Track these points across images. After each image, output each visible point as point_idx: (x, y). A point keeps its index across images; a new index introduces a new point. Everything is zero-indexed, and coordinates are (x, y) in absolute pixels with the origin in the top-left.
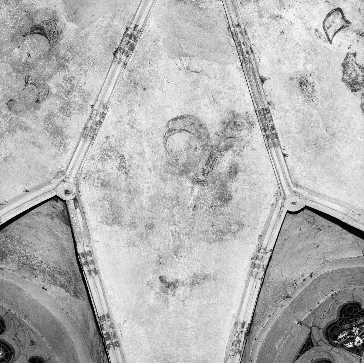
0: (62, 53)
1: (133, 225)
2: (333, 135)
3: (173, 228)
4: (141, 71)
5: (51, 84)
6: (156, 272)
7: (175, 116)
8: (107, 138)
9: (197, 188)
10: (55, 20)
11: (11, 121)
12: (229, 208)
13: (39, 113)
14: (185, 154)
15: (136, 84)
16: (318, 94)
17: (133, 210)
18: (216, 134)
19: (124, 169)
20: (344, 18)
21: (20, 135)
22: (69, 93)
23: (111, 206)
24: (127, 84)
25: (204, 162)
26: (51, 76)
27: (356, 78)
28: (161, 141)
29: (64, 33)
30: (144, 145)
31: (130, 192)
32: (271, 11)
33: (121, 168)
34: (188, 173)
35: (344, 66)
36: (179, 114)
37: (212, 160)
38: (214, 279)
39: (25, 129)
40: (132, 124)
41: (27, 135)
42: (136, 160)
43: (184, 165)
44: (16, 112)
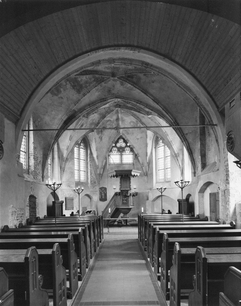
1: (131, 134)
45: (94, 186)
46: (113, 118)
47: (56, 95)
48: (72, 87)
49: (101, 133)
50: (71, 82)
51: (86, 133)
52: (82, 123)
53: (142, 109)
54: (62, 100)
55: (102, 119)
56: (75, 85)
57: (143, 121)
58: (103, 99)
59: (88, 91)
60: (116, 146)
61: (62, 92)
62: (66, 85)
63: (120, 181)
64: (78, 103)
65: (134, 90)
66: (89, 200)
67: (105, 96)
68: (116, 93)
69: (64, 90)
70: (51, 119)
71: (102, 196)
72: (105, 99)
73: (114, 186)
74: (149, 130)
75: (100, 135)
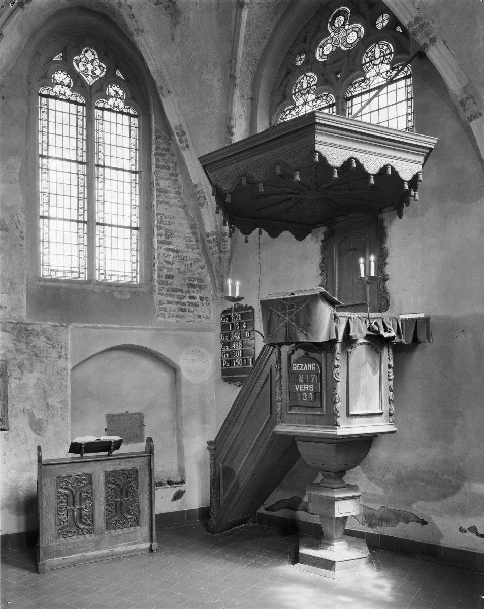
45: (187, 300)
60: (311, 64)
63: (321, 257)
66: (163, 376)
71: (231, 354)
73: (229, 281)
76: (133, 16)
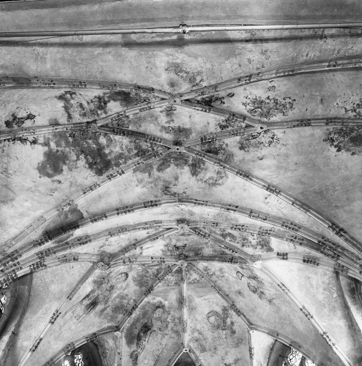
0: (167, 310)
1: (210, 350)
2: (255, 307)
3: (222, 347)
4: (192, 304)
5: (168, 320)
6: (223, 363)
7: (208, 313)
8: (191, 327)
9: (224, 332)
10: (161, 303)
11: (162, 334)
12: (236, 335)
13: (169, 329)
14: (216, 322)
15: (192, 308)
16: (245, 295)
17: (208, 345)
18: (222, 314)
19: (200, 333)
20: (241, 274)
21: (166, 337)
22: (174, 320)
23: (201, 346)
24: (189, 310)
25: (222, 323)
26: (167, 317)
27: (253, 289)
28: (207, 321)
29: (166, 304)
30: (203, 324)
31: (205, 340)
32: (220, 275)
33: (199, 333)
34: (219, 328)
35: (248, 286)
36: (209, 312)
37: (224, 322)
38: (241, 360)
39: (167, 334)
40: (196, 320)
41: (168, 336)
42: (202, 329)
43: (217, 325)
44: (163, 331)
46: (169, 298)
47: (49, 176)
48: (87, 166)
49: (138, 344)
50: (89, 157)
51: (99, 331)
52: (96, 294)
53: (238, 249)
54: (59, 185)
55: (144, 296)
56: (95, 163)
57: (238, 307)
58: (151, 202)
59: (120, 171)
61: (65, 172)
62: (76, 161)
64: (92, 189)
65: (220, 184)
67: (156, 196)
68: (182, 193)
69: (70, 170)
70: (17, 215)
72: (156, 201)
74: (256, 329)
75: (134, 347)
76: (121, 359)
